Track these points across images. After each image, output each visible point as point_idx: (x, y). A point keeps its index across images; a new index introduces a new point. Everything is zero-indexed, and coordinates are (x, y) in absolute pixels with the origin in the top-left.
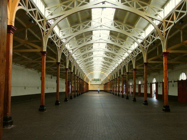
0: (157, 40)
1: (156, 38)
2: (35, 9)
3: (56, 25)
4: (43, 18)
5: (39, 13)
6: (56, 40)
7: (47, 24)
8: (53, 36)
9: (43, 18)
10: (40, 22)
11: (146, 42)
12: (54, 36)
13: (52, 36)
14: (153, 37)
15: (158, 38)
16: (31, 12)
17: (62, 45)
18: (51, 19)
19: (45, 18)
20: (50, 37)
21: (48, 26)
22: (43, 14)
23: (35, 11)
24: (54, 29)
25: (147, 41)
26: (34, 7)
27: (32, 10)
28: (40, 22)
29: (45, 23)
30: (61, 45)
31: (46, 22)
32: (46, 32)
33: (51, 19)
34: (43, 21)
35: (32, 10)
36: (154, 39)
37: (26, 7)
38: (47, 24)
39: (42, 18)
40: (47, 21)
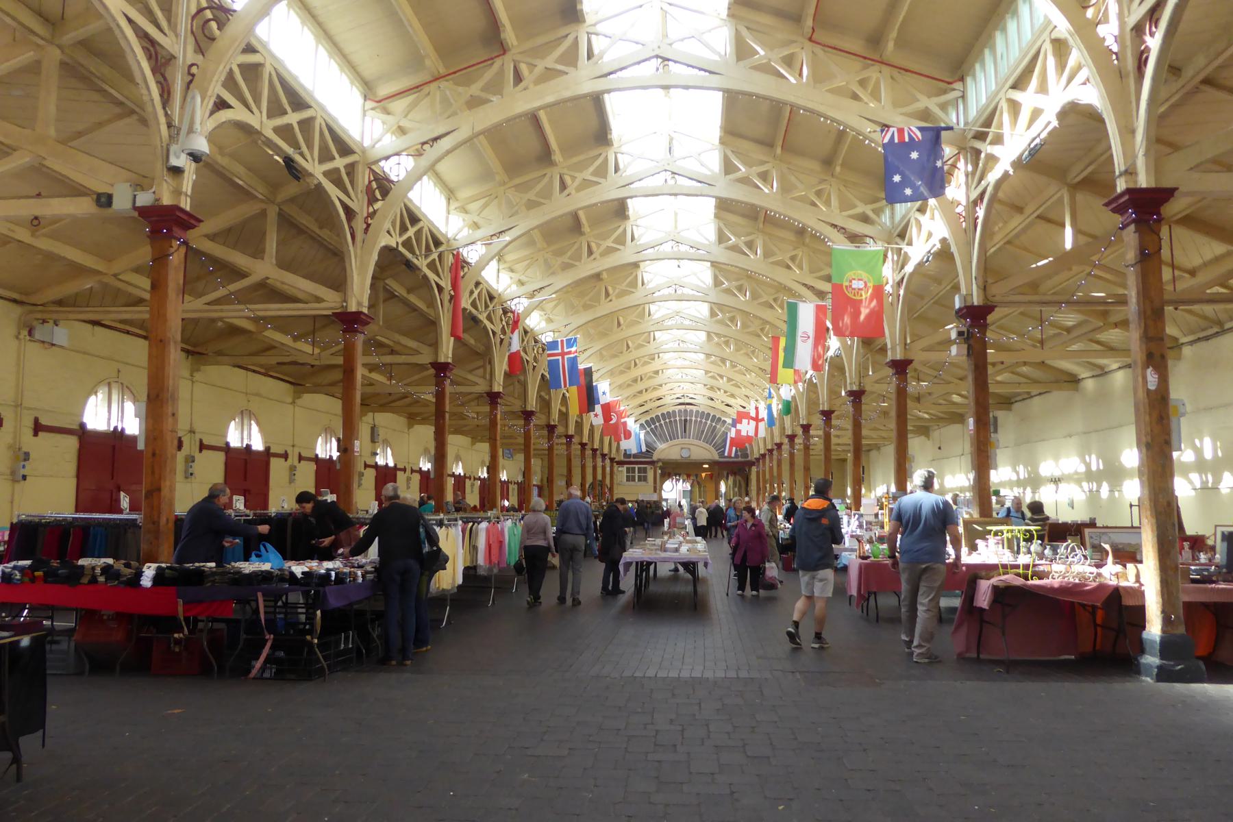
3: (425, 173)
4: (353, 152)
5: (331, 130)
8: (411, 232)
9: (353, 152)
13: (405, 237)
16: (285, 132)
19: (364, 151)
21: (382, 186)
23: (306, 124)
27: (293, 118)
29: (363, 178)
31: (367, 171)
34: (351, 169)
35: (293, 118)
40: (370, 165)
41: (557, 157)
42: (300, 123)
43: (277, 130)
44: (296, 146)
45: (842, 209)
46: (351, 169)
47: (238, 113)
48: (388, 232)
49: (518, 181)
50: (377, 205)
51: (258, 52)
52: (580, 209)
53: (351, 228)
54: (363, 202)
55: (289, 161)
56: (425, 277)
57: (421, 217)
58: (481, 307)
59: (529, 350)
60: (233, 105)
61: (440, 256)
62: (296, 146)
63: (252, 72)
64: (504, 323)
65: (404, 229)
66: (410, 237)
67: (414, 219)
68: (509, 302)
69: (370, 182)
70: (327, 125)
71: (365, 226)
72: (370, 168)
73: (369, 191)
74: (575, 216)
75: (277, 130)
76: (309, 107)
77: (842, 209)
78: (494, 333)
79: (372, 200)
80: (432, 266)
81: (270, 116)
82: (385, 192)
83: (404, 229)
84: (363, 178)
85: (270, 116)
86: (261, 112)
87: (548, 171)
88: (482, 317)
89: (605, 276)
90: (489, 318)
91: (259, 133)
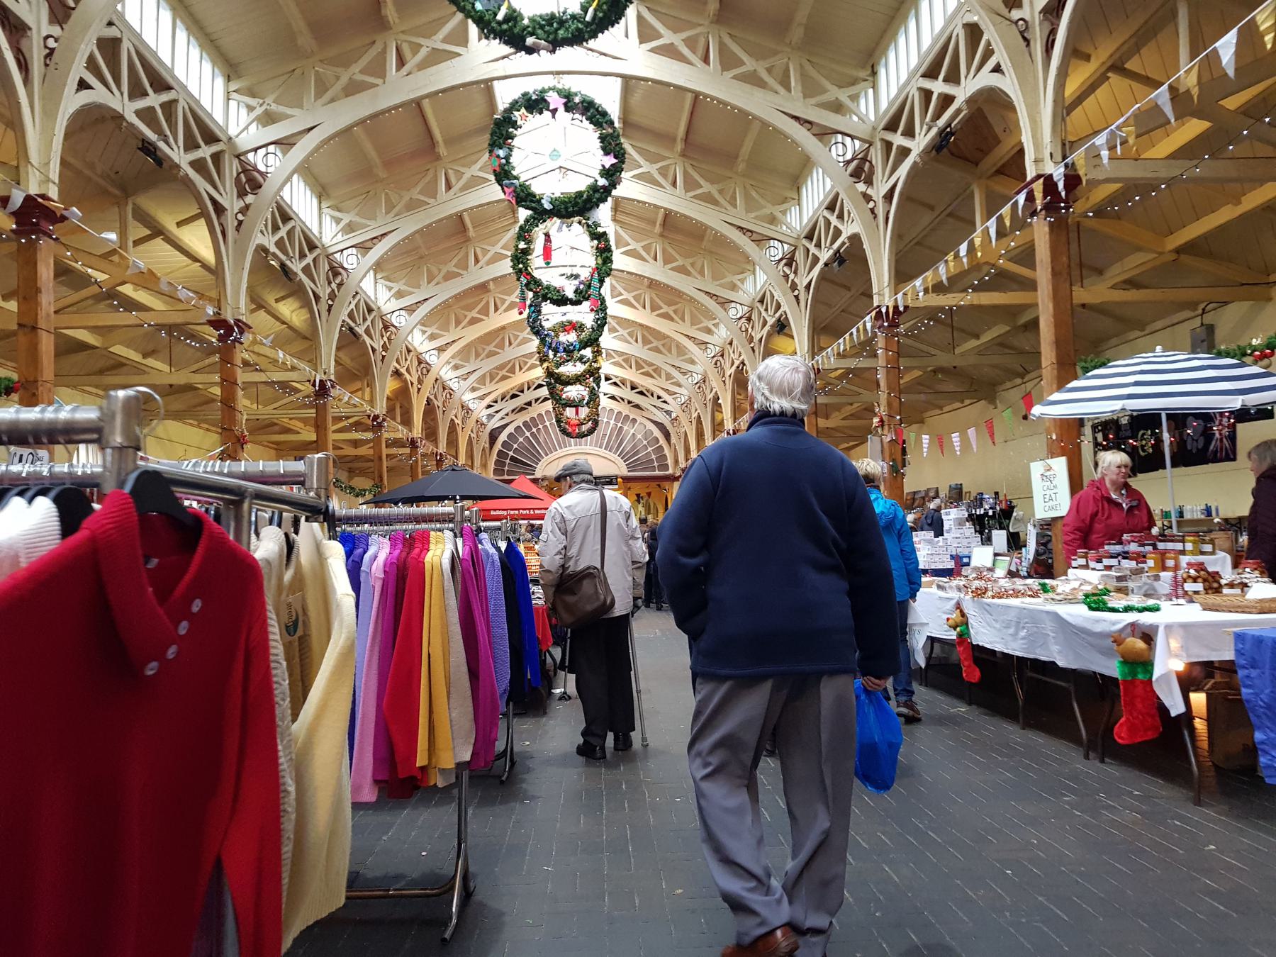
0: (970, 101)
1: (963, 93)
2: (165, 97)
4: (218, 140)
6: (302, 256)
7: (245, 171)
8: (283, 233)
9: (218, 140)
11: (888, 145)
14: (939, 87)
15: (986, 79)
16: (147, 115)
17: (340, 285)
18: (266, 146)
21: (250, 181)
22: (218, 116)
23: (169, 107)
26: (161, 85)
27: (154, 100)
28: (198, 165)
29: (231, 168)
31: (236, 162)
32: (240, 217)
33: (266, 146)
34: (216, 157)
36: (947, 100)
38: (245, 171)
39: (211, 138)
41: (442, 150)
42: (162, 105)
43: (139, 113)
44: (160, 132)
45: (692, 324)
46: (216, 157)
47: (99, 95)
48: (262, 232)
50: (250, 199)
51: (172, 88)
52: (466, 210)
53: (221, 225)
54: (232, 195)
55: (283, 265)
56: (301, 283)
57: (293, 216)
58: (360, 320)
59: (439, 397)
60: (94, 86)
61: (314, 260)
63: (110, 47)
64: (385, 339)
66: (282, 237)
67: (286, 218)
68: (388, 316)
69: (238, 174)
71: (236, 224)
74: (459, 217)
75: (139, 113)
76: (170, 88)
77: (692, 324)
78: (374, 350)
79: (242, 194)
80: (306, 270)
81: (132, 96)
82: (256, 186)
83: (276, 228)
84: (231, 168)
85: (132, 96)
86: (122, 94)
87: (485, 296)
88: (360, 330)
89: (492, 286)
90: (367, 332)
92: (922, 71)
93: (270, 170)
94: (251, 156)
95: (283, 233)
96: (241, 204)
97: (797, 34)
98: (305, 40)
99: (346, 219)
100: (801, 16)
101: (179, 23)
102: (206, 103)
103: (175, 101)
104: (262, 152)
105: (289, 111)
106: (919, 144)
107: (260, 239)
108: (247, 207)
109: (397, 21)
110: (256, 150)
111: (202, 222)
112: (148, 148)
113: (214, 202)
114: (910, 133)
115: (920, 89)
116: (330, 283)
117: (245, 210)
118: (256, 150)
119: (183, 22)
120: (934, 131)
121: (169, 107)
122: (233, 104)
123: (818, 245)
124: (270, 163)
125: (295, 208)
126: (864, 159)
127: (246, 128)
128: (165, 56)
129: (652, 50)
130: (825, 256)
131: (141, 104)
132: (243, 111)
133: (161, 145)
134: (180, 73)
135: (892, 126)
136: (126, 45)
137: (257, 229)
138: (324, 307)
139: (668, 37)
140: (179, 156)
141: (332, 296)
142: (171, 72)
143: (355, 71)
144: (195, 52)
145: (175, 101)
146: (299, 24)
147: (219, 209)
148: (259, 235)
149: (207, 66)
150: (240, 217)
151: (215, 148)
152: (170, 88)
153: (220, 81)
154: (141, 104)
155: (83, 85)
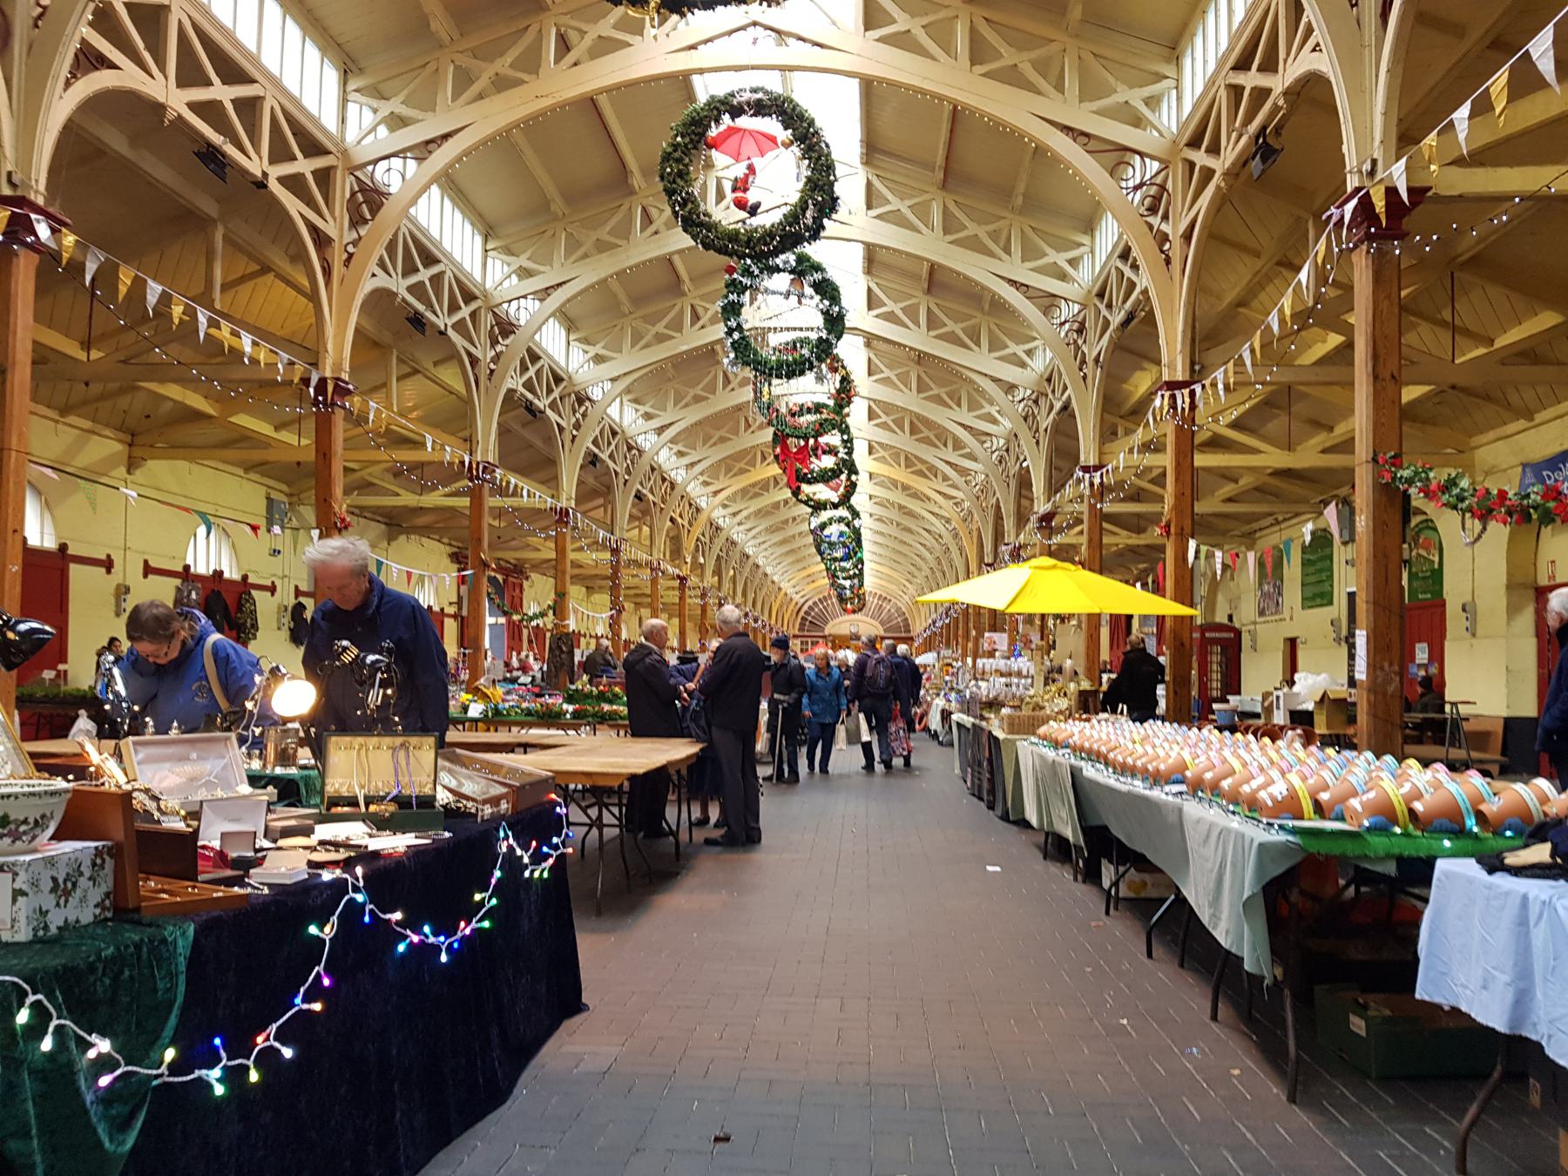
2: (435, 270)
4: (475, 298)
6: (550, 391)
8: (532, 372)
9: (475, 298)
10: (460, 327)
12: (538, 373)
17: (584, 415)
19: (486, 295)
20: (514, 382)
23: (437, 280)
24: (537, 337)
25: (1098, 304)
26: (430, 259)
27: (424, 275)
28: (460, 327)
29: (487, 320)
30: (578, 415)
31: (490, 316)
32: (492, 366)
34: (474, 315)
36: (1132, 285)
37: (395, 269)
39: (469, 297)
40: (491, 309)
41: (687, 285)
43: (410, 289)
47: (382, 281)
49: (640, 313)
50: (499, 348)
53: (475, 375)
62: (430, 306)
65: (524, 369)
67: (534, 358)
69: (492, 327)
70: (455, 276)
72: (494, 312)
73: (491, 334)
75: (410, 289)
76: (438, 261)
79: (494, 343)
83: (524, 369)
91: (396, 295)
92: (1117, 253)
93: (522, 322)
94: (505, 306)
95: (532, 372)
96: (493, 353)
97: (1020, 200)
98: (558, 206)
99: (593, 351)
100: (1021, 188)
101: (446, 199)
102: (467, 267)
103: (442, 273)
104: (515, 303)
105: (542, 268)
106: (1117, 319)
107: (510, 383)
108: (498, 356)
109: (644, 185)
110: (510, 301)
111: (455, 361)
112: (417, 321)
113: (469, 354)
114: (1109, 306)
115: (1117, 268)
116: (574, 412)
117: (497, 358)
118: (510, 301)
119: (449, 196)
120: (1123, 312)
121: (437, 280)
122: (490, 260)
123: (1053, 391)
124: (524, 312)
125: (544, 345)
126: (1082, 324)
127: (501, 284)
128: (435, 233)
129: (878, 217)
130: (1058, 405)
131: (413, 280)
132: (498, 263)
133: (429, 315)
134: (446, 245)
135: (1101, 295)
136: (404, 229)
137: (508, 375)
138: (567, 437)
139: (895, 203)
140: (442, 320)
141: (577, 426)
142: (438, 245)
143: (603, 233)
144: (458, 215)
145: (444, 272)
146: (551, 190)
147: (474, 361)
148: (510, 380)
149: (468, 227)
150: (492, 366)
151: (474, 306)
152: (438, 261)
153: (478, 240)
154: (413, 280)
155: (374, 275)
